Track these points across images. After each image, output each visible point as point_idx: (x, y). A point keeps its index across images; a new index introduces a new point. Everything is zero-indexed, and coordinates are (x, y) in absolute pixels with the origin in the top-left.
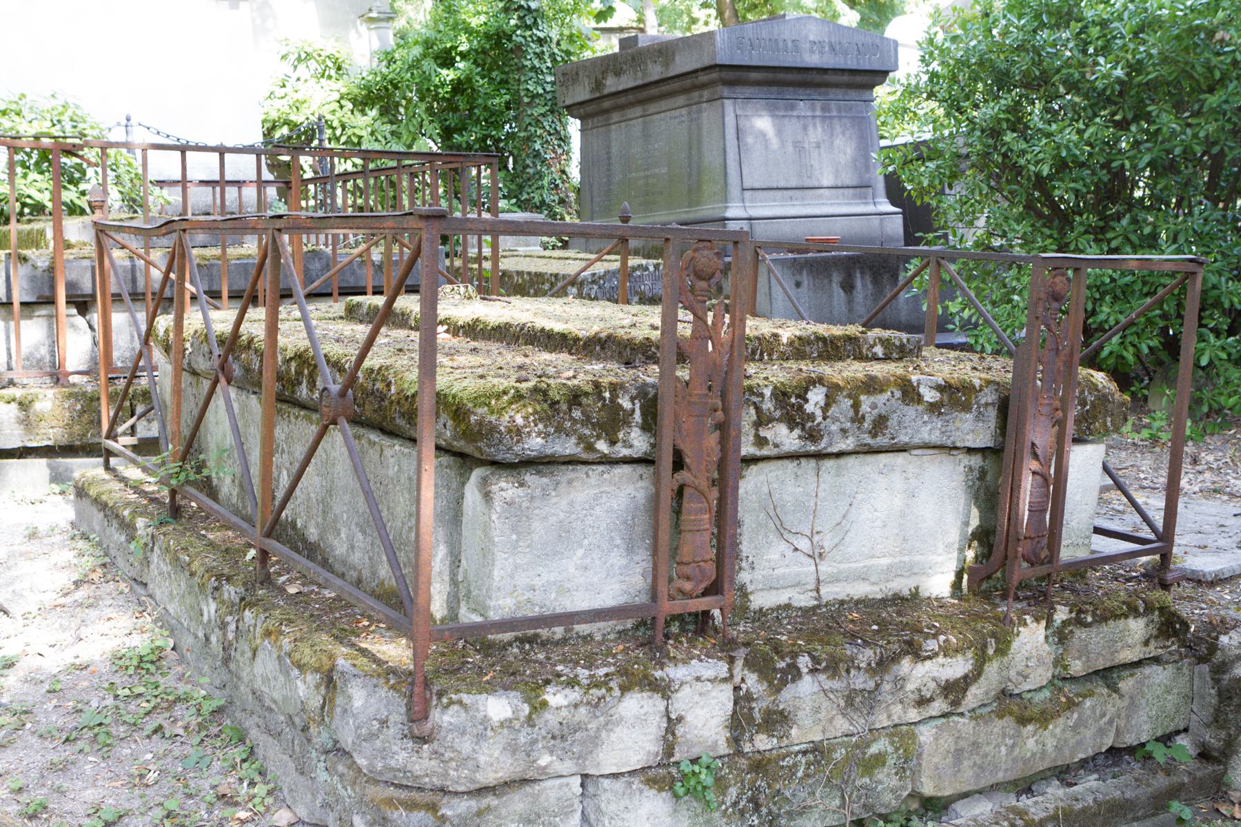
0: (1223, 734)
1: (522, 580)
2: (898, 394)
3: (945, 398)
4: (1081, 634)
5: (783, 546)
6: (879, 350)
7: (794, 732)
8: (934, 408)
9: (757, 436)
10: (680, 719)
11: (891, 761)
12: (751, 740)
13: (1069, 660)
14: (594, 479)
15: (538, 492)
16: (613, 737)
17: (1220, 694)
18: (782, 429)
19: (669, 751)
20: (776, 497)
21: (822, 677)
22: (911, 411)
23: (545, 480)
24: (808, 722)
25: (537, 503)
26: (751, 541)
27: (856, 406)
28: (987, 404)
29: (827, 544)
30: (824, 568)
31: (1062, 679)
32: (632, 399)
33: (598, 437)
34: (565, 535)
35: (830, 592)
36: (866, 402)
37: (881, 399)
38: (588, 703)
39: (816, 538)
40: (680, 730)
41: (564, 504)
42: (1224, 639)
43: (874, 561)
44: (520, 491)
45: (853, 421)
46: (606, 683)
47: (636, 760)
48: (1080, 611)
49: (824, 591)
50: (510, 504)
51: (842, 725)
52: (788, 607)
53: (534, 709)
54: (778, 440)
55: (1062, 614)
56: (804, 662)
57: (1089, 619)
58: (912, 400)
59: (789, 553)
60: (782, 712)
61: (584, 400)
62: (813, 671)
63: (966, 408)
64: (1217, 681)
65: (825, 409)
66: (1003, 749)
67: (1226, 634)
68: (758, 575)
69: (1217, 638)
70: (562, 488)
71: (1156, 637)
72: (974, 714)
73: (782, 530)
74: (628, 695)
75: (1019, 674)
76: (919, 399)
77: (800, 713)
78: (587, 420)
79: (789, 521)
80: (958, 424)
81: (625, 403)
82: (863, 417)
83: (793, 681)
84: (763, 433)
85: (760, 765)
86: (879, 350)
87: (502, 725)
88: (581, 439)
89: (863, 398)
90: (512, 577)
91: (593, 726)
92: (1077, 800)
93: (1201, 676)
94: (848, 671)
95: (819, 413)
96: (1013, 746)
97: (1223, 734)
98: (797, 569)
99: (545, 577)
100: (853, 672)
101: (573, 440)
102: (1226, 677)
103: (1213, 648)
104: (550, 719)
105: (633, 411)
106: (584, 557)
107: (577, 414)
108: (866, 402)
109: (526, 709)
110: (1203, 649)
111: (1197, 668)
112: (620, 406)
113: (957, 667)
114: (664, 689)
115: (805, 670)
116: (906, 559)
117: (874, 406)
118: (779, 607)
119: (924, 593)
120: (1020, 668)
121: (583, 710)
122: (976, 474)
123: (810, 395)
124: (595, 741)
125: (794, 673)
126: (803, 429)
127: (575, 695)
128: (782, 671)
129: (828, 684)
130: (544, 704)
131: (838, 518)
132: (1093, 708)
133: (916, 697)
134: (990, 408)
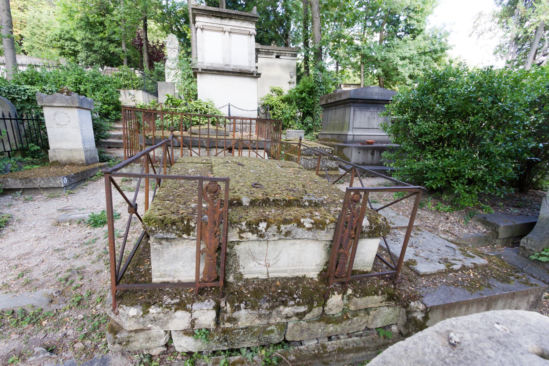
0: (407, 331)
1: (162, 269)
2: (295, 225)
3: (314, 226)
4: (355, 299)
5: (255, 263)
6: (307, 204)
7: (239, 323)
8: (309, 229)
9: (240, 236)
10: (196, 319)
11: (276, 332)
12: (224, 324)
13: (350, 305)
14: (185, 243)
15: (165, 246)
16: (173, 321)
17: (407, 319)
18: (250, 234)
19: (193, 326)
20: (252, 250)
21: (249, 310)
22: (300, 230)
23: (168, 243)
24: (244, 321)
25: (165, 249)
26: (243, 261)
27: (279, 228)
28: (331, 228)
29: (271, 263)
30: (270, 269)
31: (344, 312)
32: (195, 224)
33: (183, 234)
34: (176, 258)
35: (271, 275)
36: (283, 227)
37: (289, 226)
38: (163, 313)
39: (267, 261)
40: (196, 322)
41: (174, 250)
42: (412, 304)
43: (289, 268)
44: (159, 246)
45: (277, 232)
46: (171, 307)
47: (182, 327)
48: (355, 293)
49: (270, 275)
50: (156, 249)
51: (257, 322)
52: (257, 278)
53: (144, 314)
54: (248, 237)
55: (350, 292)
56: (242, 305)
57: (358, 296)
58: (301, 227)
59: (257, 265)
60: (234, 318)
61: (177, 224)
62: (245, 308)
63: (323, 229)
64: (407, 316)
65: (266, 229)
66: (320, 330)
67: (414, 301)
68: (246, 270)
69: (410, 302)
70: (173, 246)
71: (385, 301)
72: (308, 322)
73: (254, 259)
74: (178, 311)
75: (329, 309)
76: (304, 227)
77: (241, 319)
78: (178, 229)
79: (256, 256)
80: (319, 233)
81: (192, 224)
82: (282, 231)
83: (238, 310)
84: (241, 235)
85: (225, 331)
86: (307, 204)
87: (133, 317)
88: (176, 234)
89: (281, 226)
90: (158, 267)
91: (165, 319)
92: (346, 345)
93: (403, 311)
94: (259, 309)
95: (264, 231)
96: (324, 329)
97: (407, 331)
98: (260, 269)
99: (170, 268)
100: (260, 309)
101: (174, 234)
102: (410, 316)
103: (408, 305)
104: (150, 316)
105: (195, 227)
106: (183, 263)
107: (174, 227)
108: (283, 227)
109: (142, 313)
110: (405, 304)
111: (402, 309)
112: (191, 226)
113: (302, 309)
114: (190, 311)
115: (242, 308)
116: (301, 268)
117: (286, 228)
118: (254, 278)
119: (307, 276)
120: (330, 307)
121: (162, 315)
122: (328, 246)
123: (261, 225)
124: (167, 322)
125: (239, 308)
126: (257, 234)
127: (159, 310)
128: (236, 306)
129: (251, 312)
130: (148, 312)
131: (275, 256)
132: (357, 320)
133: (285, 316)
134: (332, 230)
